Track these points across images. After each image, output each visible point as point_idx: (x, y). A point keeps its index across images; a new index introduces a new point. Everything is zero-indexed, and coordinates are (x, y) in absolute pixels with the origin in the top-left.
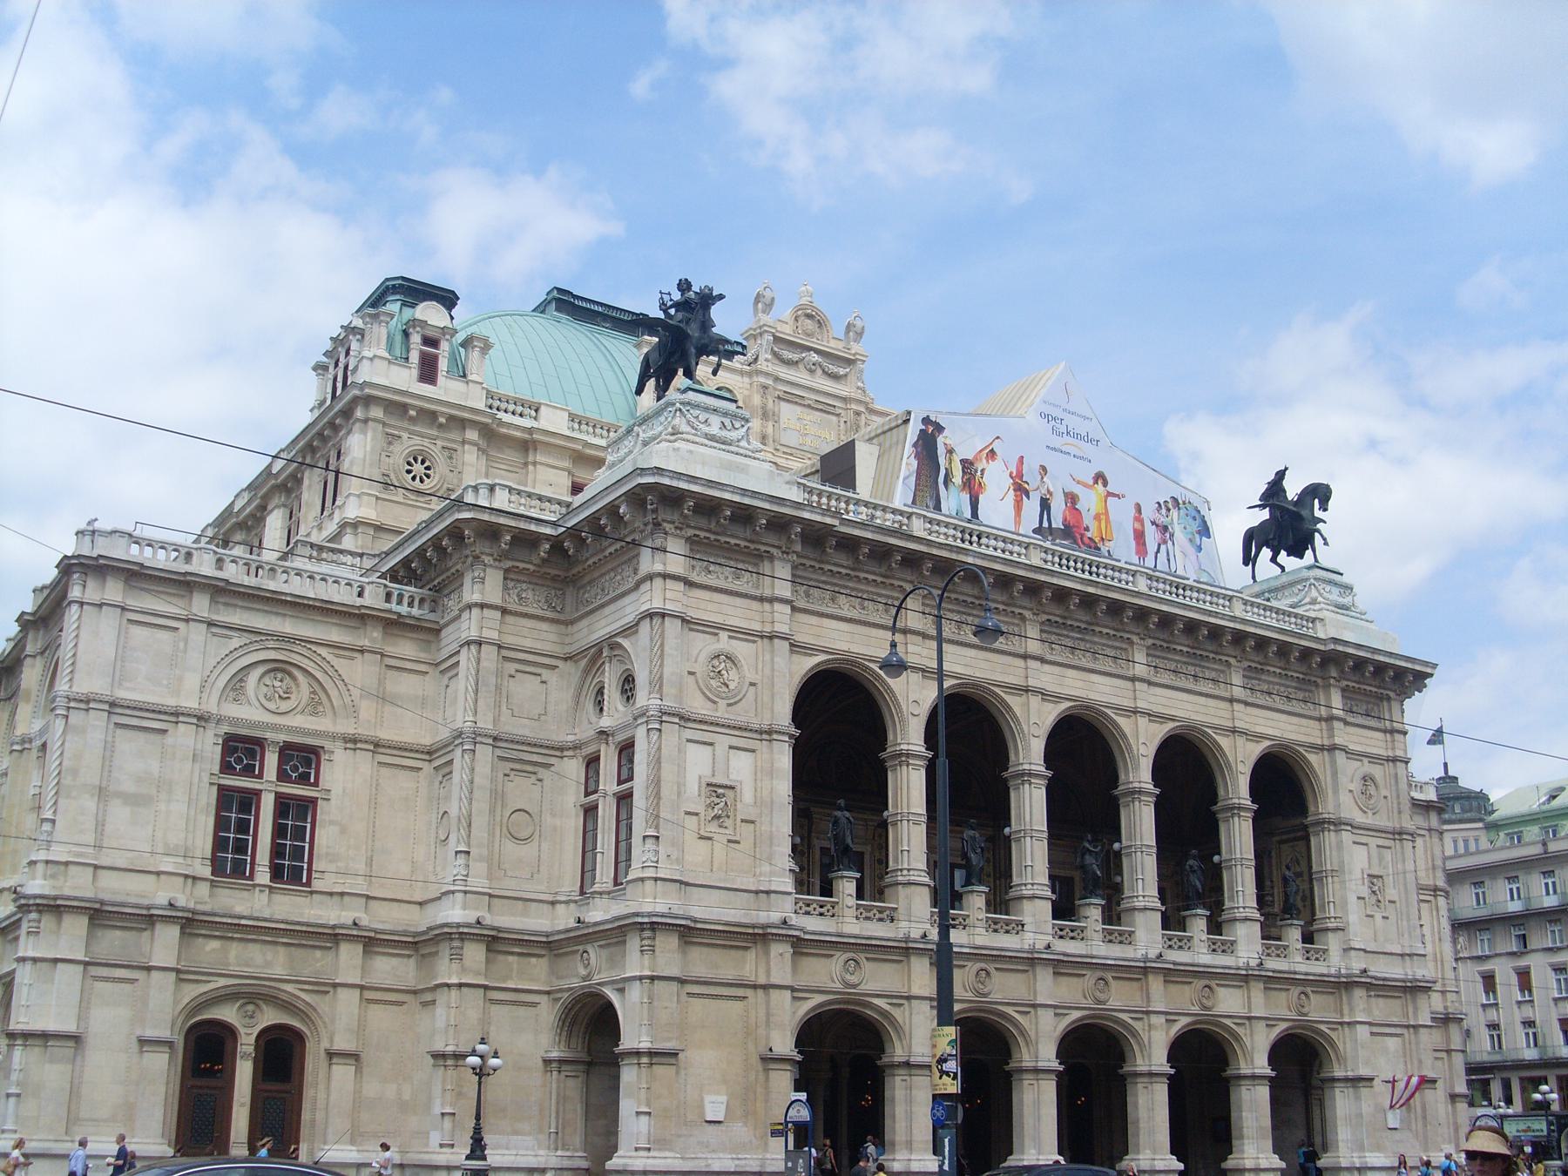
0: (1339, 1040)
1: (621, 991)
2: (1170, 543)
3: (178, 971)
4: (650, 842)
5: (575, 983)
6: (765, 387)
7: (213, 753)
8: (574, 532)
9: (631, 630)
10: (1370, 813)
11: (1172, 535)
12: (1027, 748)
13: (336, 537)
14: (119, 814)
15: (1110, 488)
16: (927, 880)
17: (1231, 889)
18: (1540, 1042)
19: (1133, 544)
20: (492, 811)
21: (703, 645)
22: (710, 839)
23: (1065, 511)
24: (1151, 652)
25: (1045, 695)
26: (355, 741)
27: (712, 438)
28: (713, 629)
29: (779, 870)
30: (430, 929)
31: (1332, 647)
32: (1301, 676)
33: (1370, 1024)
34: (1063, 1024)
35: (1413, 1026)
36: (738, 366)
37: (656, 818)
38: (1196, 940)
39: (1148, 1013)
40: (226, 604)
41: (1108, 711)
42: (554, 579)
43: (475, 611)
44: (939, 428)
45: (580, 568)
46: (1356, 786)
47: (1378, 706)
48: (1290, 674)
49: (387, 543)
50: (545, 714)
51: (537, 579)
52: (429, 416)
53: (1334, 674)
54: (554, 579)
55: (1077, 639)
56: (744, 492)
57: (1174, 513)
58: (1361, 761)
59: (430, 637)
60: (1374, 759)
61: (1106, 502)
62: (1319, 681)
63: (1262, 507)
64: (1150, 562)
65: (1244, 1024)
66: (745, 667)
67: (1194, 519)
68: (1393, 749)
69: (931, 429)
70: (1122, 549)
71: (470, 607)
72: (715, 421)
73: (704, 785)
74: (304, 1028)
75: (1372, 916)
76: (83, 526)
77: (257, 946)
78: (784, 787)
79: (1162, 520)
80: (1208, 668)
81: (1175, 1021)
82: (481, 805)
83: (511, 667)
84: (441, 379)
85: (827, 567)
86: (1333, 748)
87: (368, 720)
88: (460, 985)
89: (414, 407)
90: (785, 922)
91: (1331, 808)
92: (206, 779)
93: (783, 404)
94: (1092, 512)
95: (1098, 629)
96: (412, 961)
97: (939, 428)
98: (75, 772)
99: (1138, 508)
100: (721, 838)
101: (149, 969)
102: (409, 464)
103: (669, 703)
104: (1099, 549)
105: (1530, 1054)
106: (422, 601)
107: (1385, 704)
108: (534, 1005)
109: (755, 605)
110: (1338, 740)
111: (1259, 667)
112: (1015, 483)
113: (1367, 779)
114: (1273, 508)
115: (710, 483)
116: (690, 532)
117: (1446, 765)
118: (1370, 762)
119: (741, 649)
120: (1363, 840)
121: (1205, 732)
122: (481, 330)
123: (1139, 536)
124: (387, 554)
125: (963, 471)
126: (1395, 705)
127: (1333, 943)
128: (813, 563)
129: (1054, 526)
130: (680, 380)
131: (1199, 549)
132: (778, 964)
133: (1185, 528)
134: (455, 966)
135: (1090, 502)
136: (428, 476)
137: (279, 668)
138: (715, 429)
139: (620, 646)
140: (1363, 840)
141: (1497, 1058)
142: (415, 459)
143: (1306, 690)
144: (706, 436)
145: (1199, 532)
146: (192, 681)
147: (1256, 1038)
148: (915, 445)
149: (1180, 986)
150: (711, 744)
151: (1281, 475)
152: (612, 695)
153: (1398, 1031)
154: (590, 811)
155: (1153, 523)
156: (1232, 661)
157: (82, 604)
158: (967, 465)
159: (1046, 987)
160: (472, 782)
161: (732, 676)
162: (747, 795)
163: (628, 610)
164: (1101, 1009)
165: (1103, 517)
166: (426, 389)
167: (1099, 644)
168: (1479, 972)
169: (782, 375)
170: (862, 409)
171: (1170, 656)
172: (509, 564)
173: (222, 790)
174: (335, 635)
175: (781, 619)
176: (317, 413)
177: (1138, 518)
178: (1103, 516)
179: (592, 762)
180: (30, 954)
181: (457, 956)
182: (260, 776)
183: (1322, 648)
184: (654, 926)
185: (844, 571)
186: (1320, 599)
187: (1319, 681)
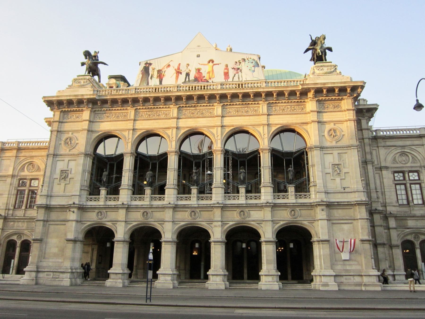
11: (241, 71)
15: (214, 63)
19: (223, 77)
23: (195, 74)
44: (150, 64)
56: (67, 96)
57: (243, 63)
61: (213, 67)
64: (230, 80)
67: (252, 63)
73: (60, 171)
81: (228, 224)
94: (207, 71)
97: (150, 64)
99: (227, 66)
104: (208, 82)
112: (177, 71)
123: (226, 74)
125: (158, 73)
129: (190, 79)
133: (247, 66)
145: (254, 66)
148: (142, 71)
149: (232, 212)
150: (64, 160)
153: (350, 221)
155: (234, 68)
158: (159, 71)
162: (73, 172)
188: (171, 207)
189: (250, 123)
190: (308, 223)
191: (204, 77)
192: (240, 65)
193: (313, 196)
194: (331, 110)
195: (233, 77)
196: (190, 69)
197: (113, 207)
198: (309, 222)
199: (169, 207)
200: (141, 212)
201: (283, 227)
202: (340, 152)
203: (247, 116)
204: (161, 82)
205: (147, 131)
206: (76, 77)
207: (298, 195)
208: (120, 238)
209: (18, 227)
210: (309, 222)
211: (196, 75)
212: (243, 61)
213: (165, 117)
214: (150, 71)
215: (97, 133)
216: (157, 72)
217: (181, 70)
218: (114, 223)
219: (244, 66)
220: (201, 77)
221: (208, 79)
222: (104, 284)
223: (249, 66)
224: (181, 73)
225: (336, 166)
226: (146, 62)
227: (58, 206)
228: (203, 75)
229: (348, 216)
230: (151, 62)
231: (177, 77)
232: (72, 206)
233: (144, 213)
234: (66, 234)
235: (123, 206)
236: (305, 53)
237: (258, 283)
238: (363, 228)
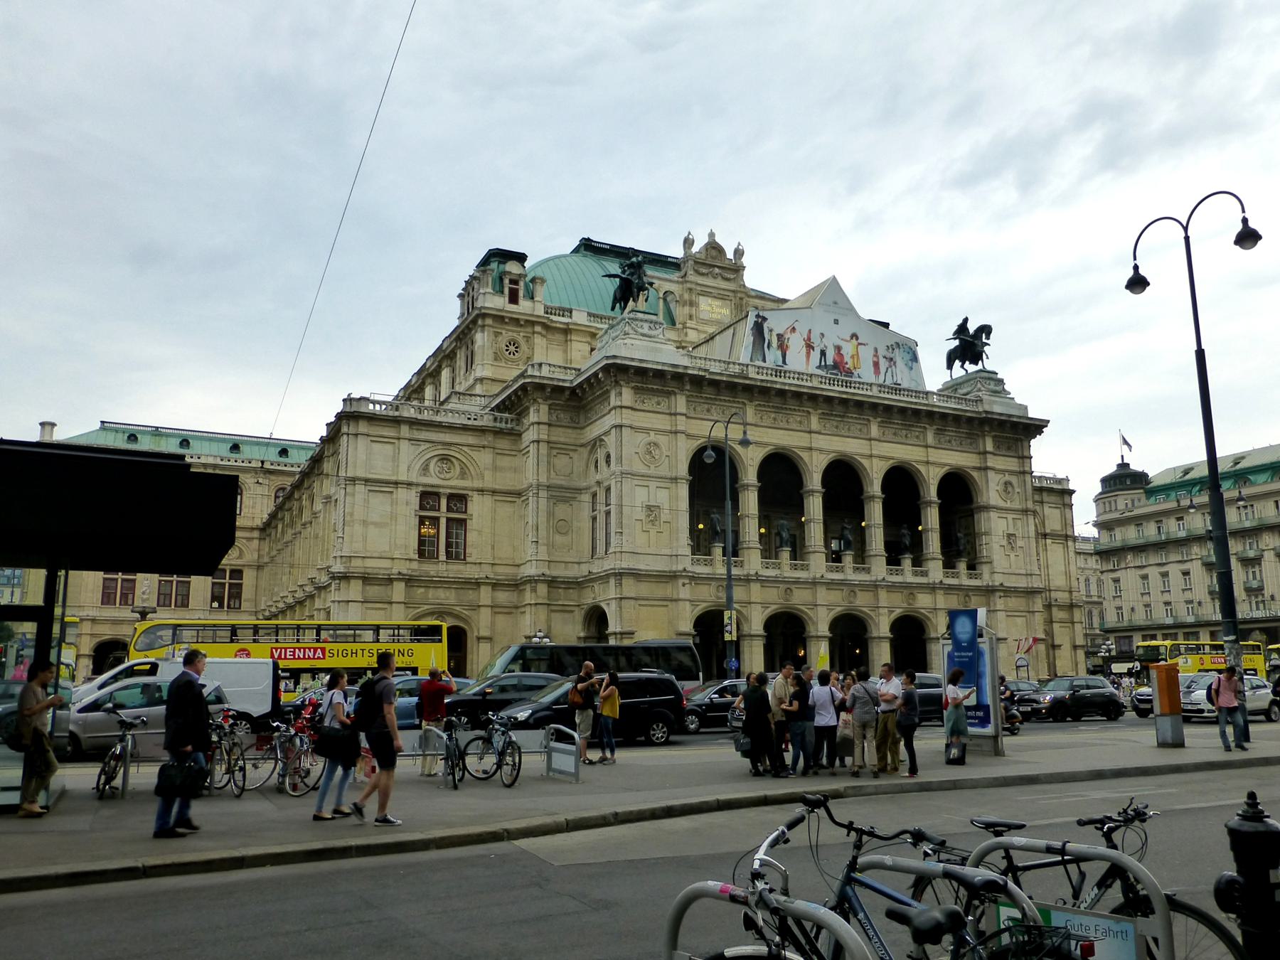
1: (608, 604)
3: (405, 603)
4: (618, 534)
5: (590, 601)
6: (691, 289)
7: (415, 501)
8: (580, 385)
9: (607, 433)
10: (1009, 501)
11: (895, 363)
12: (812, 478)
13: (472, 386)
14: (372, 531)
15: (859, 341)
16: (759, 546)
17: (926, 544)
18: (1174, 614)
19: (872, 369)
20: (548, 521)
21: (642, 439)
25: (821, 451)
26: (483, 491)
27: (643, 335)
28: (647, 430)
29: (683, 542)
30: (521, 578)
31: (984, 415)
33: (1006, 611)
34: (832, 615)
35: (1033, 612)
36: (676, 279)
37: (621, 524)
38: (906, 570)
39: (878, 607)
40: (418, 430)
42: (574, 407)
43: (536, 426)
44: (765, 319)
45: (585, 402)
46: (1000, 488)
49: (496, 388)
50: (572, 473)
51: (565, 408)
52: (516, 322)
53: (987, 429)
54: (574, 407)
57: (897, 350)
59: (517, 438)
60: (1012, 473)
62: (979, 433)
63: (955, 339)
66: (664, 448)
68: (1023, 466)
69: (760, 320)
70: (866, 373)
71: (533, 424)
72: (646, 325)
74: (462, 625)
76: (346, 397)
77: (441, 590)
78: (684, 504)
82: (543, 519)
83: (554, 452)
84: (521, 301)
86: (986, 468)
87: (488, 482)
88: (536, 604)
89: (507, 317)
90: (685, 570)
91: (985, 500)
92: (413, 513)
93: (701, 297)
94: (850, 354)
95: (850, 415)
96: (515, 593)
97: (765, 319)
98: (352, 514)
99: (876, 350)
101: (391, 603)
102: (507, 346)
103: (625, 468)
105: (1169, 621)
106: (512, 420)
107: (1019, 443)
108: (572, 612)
109: (668, 417)
110: (989, 464)
112: (806, 344)
113: (1007, 484)
114: (961, 340)
115: (641, 361)
116: (633, 384)
117: (1122, 456)
119: (662, 440)
120: (1004, 515)
122: (539, 273)
123: (876, 365)
124: (497, 395)
125: (778, 340)
126: (1025, 444)
127: (985, 570)
130: (631, 303)
131: (911, 368)
132: (685, 592)
134: (533, 594)
135: (848, 349)
136: (517, 352)
137: (444, 459)
138: (646, 331)
139: (603, 440)
140: (1004, 515)
141: (1149, 623)
142: (510, 344)
146: (403, 467)
147: (939, 619)
148: (752, 329)
150: (647, 486)
151: (966, 320)
152: (602, 463)
153: (1024, 614)
154: (594, 519)
155: (885, 357)
156: (927, 426)
157: (348, 434)
158: (780, 336)
160: (538, 508)
161: (656, 453)
163: (607, 423)
165: (855, 357)
166: (513, 307)
168: (1112, 579)
169: (699, 282)
170: (743, 295)
172: (551, 402)
173: (421, 517)
174: (471, 439)
175: (682, 423)
176: (461, 320)
177: (876, 355)
178: (856, 356)
179: (594, 495)
180: (337, 599)
181: (534, 590)
182: (439, 510)
183: (978, 416)
184: (621, 574)
186: (983, 389)
193: (986, 576)
202: (1015, 516)
233: (786, 591)
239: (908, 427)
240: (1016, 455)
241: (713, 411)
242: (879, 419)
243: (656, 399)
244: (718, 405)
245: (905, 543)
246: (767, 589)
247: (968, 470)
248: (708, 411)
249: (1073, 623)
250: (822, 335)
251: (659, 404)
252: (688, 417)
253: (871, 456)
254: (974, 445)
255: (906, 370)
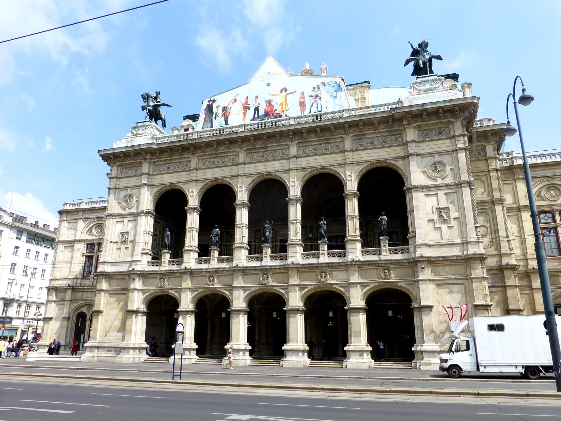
0: (414, 290)
2: (319, 101)
11: (320, 98)
15: (288, 92)
19: (299, 108)
22: (120, 248)
24: (300, 145)
28: (126, 188)
32: (389, 130)
41: (277, 174)
44: (214, 101)
47: (448, 127)
48: (380, 131)
55: (264, 151)
57: (322, 88)
58: (434, 156)
61: (286, 97)
62: (402, 128)
65: (348, 286)
67: (334, 87)
73: (120, 233)
75: (440, 228)
79: (314, 94)
80: (333, 143)
85: (162, 159)
94: (279, 104)
95: (270, 145)
97: (214, 101)
100: (123, 247)
104: (280, 116)
107: (451, 126)
111: (361, 133)
118: (439, 155)
121: (329, 169)
123: (302, 104)
128: (158, 160)
129: (260, 114)
133: (328, 92)
143: (396, 135)
144: (136, 135)
145: (336, 91)
148: (205, 110)
150: (123, 221)
158: (224, 109)
159: (239, 282)
164: (265, 286)
167: (275, 150)
171: (311, 144)
185: (168, 159)
187: (402, 128)
188: (240, 270)
189: (331, 163)
190: (406, 284)
191: (276, 110)
192: (319, 91)
193: (411, 250)
194: (434, 138)
195: (311, 107)
196: (259, 103)
197: (176, 273)
198: (406, 283)
199: (237, 270)
200: (206, 277)
201: (375, 290)
203: (328, 154)
204: (226, 123)
205: (211, 182)
206: (135, 125)
207: (393, 250)
208: (183, 308)
209: (87, 298)
210: (406, 283)
211: (267, 110)
212: (322, 86)
213: (232, 164)
214: (213, 109)
215: (157, 187)
216: (222, 110)
217: (249, 105)
218: (177, 290)
219: (324, 93)
220: (272, 111)
221: (280, 113)
222: (168, 361)
223: (330, 92)
224: (249, 108)
225: (442, 210)
226: (209, 99)
227: (118, 274)
228: (275, 108)
229: (459, 275)
230: (215, 98)
231: (245, 113)
232: (132, 272)
234: (126, 304)
235: (186, 271)
236: (405, 66)
237: (343, 361)
238: (477, 290)
239: (327, 141)
240: (448, 137)
241: (171, 167)
242: (296, 142)
243: (135, 169)
244: (175, 163)
245: (321, 233)
246: (197, 278)
247: (391, 162)
248: (168, 168)
249: (505, 287)
250: (257, 97)
251: (136, 171)
252: (149, 174)
253: (289, 170)
254: (400, 140)
255: (331, 100)
